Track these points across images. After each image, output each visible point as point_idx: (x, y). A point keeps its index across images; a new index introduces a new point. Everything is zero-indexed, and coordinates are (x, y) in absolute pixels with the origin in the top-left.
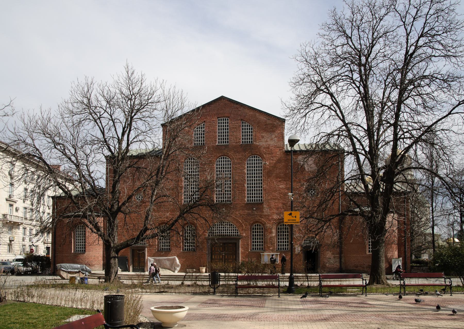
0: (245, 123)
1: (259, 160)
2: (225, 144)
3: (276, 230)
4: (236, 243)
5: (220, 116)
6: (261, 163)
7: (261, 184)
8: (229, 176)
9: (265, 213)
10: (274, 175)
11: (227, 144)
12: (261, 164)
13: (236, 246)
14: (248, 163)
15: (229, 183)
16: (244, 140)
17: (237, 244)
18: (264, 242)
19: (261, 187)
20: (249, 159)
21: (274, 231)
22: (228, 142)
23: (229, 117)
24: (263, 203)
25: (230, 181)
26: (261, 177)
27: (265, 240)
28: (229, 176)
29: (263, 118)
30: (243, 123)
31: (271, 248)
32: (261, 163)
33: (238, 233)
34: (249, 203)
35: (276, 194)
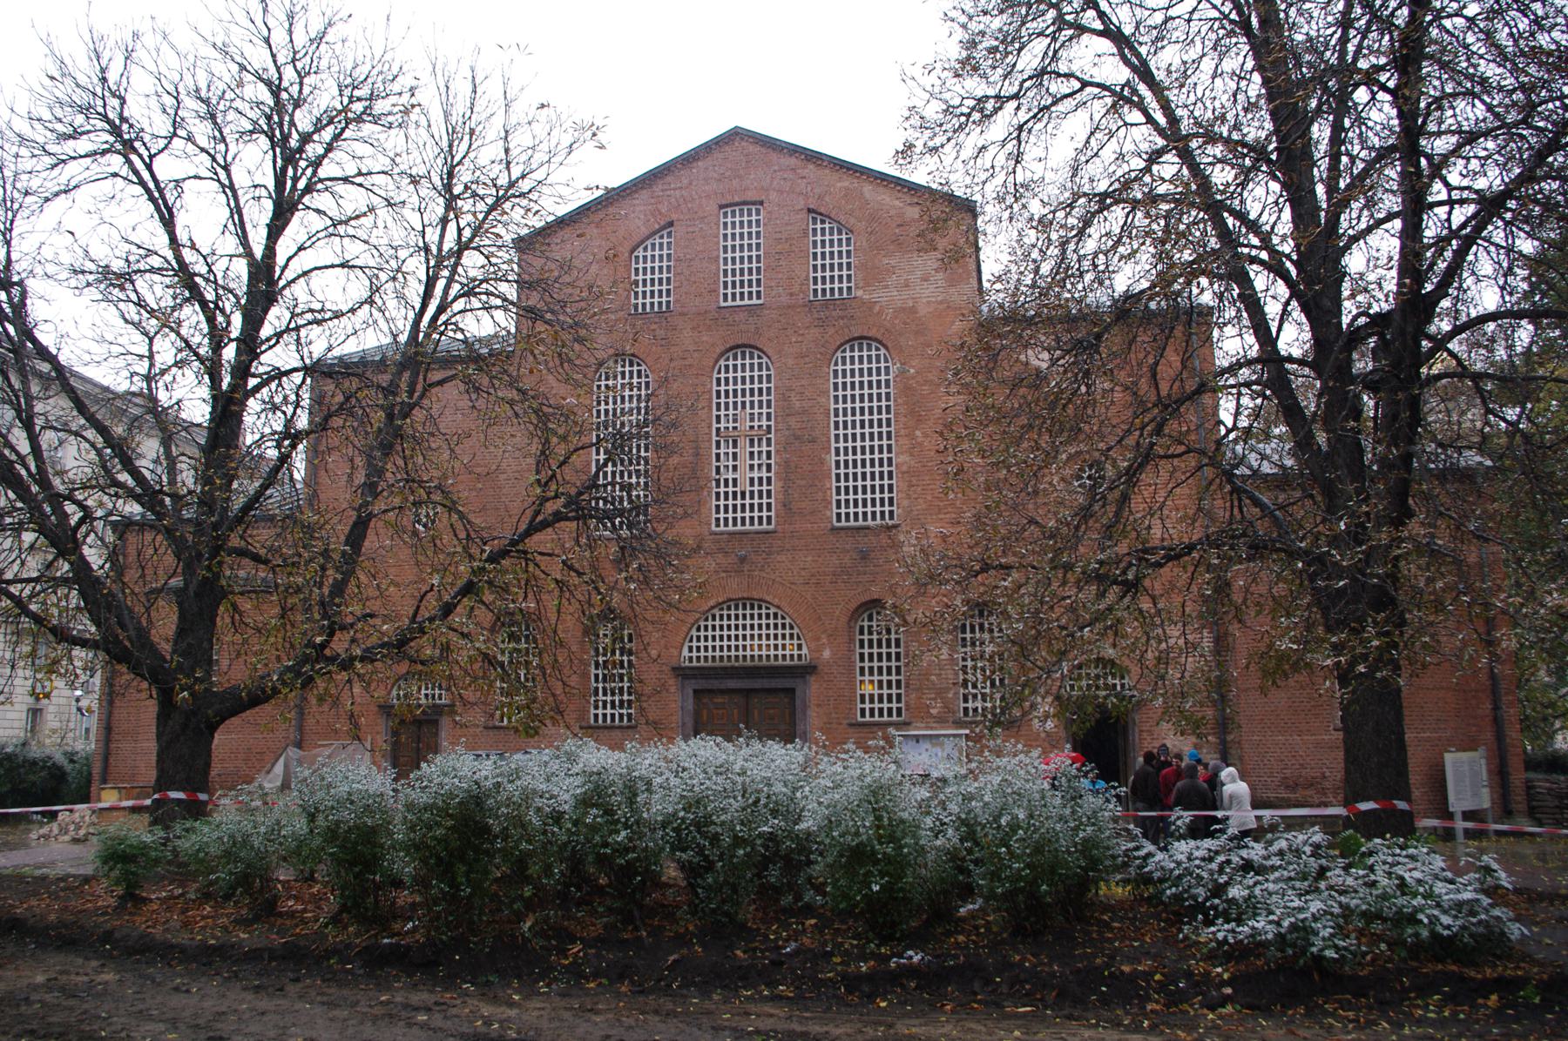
0: (823, 222)
1: (878, 356)
2: (746, 302)
4: (792, 691)
5: (729, 199)
8: (764, 423)
11: (755, 301)
12: (887, 374)
13: (793, 699)
15: (765, 449)
16: (819, 287)
17: (798, 693)
18: (907, 686)
20: (839, 354)
22: (759, 297)
23: (761, 203)
25: (769, 445)
28: (764, 423)
30: (815, 223)
32: (887, 368)
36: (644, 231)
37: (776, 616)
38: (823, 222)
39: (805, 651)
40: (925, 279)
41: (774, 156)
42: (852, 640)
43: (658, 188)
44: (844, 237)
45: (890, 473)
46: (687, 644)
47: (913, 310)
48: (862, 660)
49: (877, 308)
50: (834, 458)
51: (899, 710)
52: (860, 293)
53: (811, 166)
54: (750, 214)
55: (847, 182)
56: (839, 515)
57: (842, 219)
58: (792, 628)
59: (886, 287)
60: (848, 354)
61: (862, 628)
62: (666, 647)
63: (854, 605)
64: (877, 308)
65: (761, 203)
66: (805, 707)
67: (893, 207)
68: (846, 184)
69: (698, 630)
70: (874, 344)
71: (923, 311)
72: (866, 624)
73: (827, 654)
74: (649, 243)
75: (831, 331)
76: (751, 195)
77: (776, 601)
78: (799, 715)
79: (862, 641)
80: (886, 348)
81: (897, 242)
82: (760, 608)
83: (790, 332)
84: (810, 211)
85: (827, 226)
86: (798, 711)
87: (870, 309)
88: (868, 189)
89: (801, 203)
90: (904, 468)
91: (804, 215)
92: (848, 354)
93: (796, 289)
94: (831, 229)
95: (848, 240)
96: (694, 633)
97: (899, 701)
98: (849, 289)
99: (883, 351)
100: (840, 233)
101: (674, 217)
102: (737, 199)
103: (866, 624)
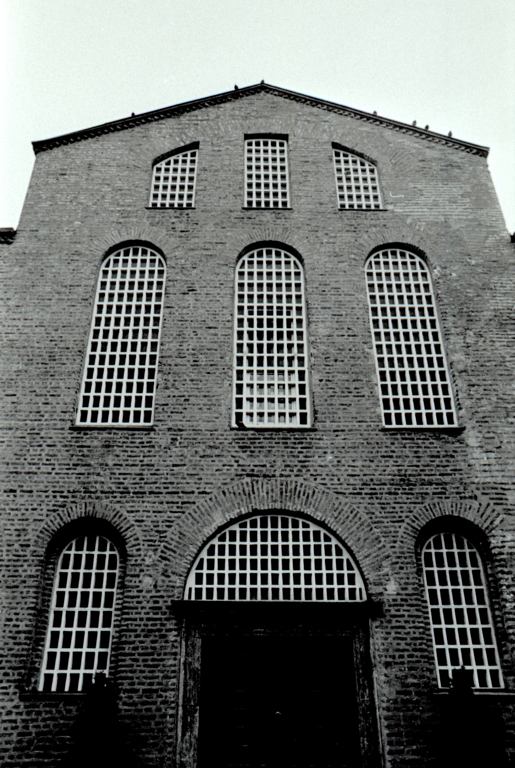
9: (481, 478)
10: (488, 314)
20: (372, 259)
24: (461, 430)
33: (352, 580)
36: (168, 147)
37: (317, 535)
39: (359, 584)
42: (419, 572)
43: (185, 118)
46: (194, 572)
47: (446, 224)
49: (409, 221)
50: (376, 356)
52: (390, 207)
53: (333, 115)
56: (388, 417)
58: (339, 552)
61: (428, 556)
62: (165, 574)
65: (285, 137)
68: (366, 129)
69: (211, 552)
73: (392, 588)
74: (172, 159)
77: (319, 516)
82: (295, 524)
83: (319, 234)
89: (325, 137)
90: (461, 367)
93: (325, 199)
96: (204, 555)
101: (200, 139)
102: (262, 131)
103: (433, 551)
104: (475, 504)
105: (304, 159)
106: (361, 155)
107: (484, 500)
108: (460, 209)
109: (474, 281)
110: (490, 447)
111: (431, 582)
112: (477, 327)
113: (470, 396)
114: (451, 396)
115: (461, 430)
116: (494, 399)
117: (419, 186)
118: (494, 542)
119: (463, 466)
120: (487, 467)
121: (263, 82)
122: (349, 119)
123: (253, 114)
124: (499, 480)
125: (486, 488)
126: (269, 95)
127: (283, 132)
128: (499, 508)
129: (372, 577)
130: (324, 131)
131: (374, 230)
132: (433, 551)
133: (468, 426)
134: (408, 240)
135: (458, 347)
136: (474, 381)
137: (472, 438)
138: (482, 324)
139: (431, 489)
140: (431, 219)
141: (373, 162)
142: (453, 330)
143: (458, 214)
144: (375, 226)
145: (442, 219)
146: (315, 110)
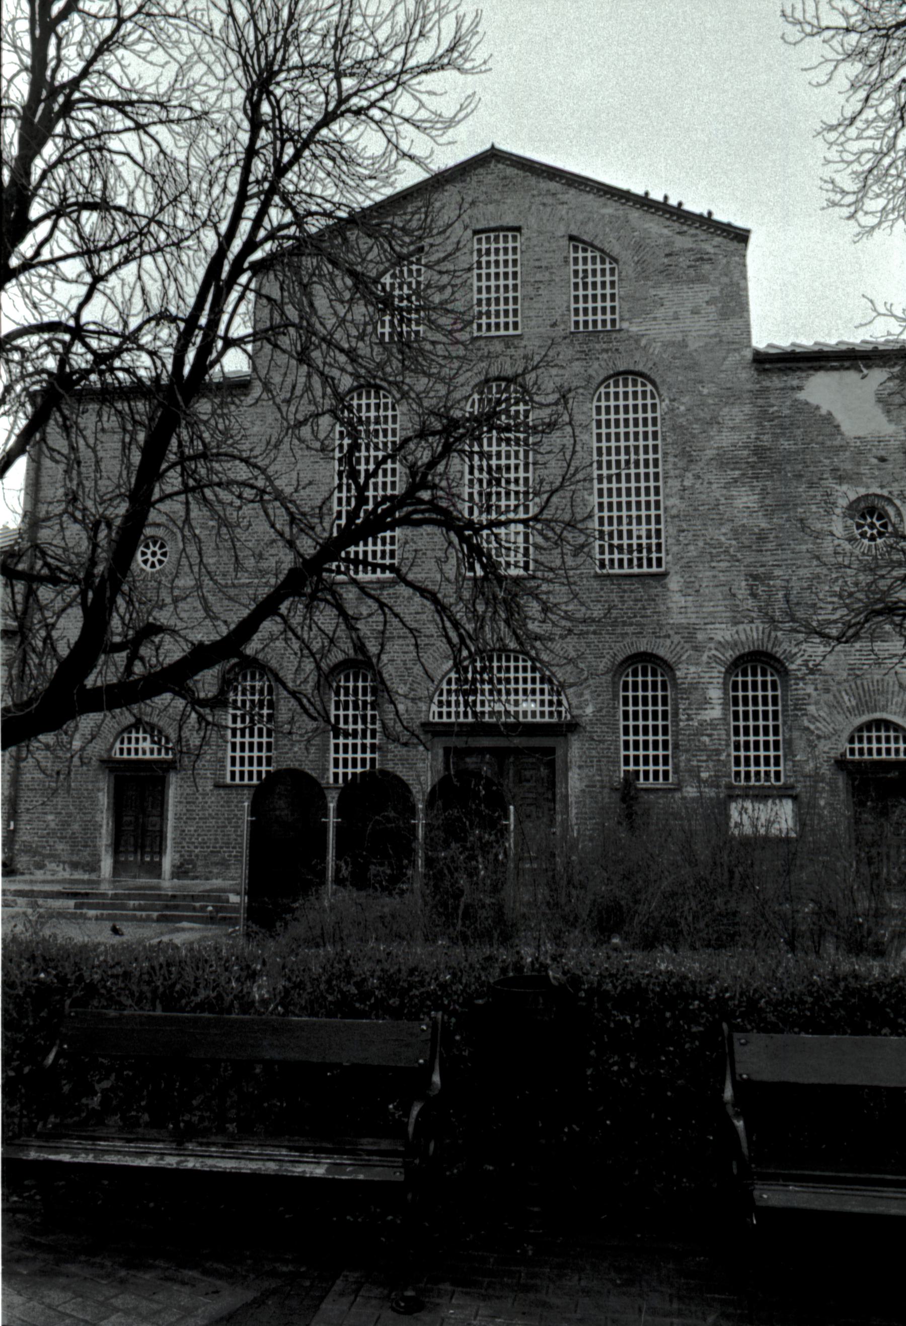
1: (644, 393)
2: (502, 332)
3: (725, 692)
4: (552, 751)
6: (654, 406)
7: (657, 493)
10: (710, 453)
11: (511, 332)
14: (598, 408)
17: (559, 752)
18: (676, 746)
19: (657, 507)
20: (602, 390)
21: (715, 694)
24: (665, 575)
26: (656, 465)
27: (676, 733)
29: (656, 228)
31: (704, 775)
32: (654, 406)
34: (609, 576)
35: (721, 534)
38: (585, 250)
40: (695, 312)
41: (533, 180)
42: (615, 696)
44: (607, 266)
45: (658, 517)
47: (683, 344)
48: (626, 718)
51: (666, 773)
52: (625, 325)
53: (572, 191)
54: (506, 241)
55: (610, 209)
57: (607, 247)
59: (655, 319)
60: (612, 390)
61: (626, 684)
63: (620, 658)
64: (643, 342)
65: (518, 229)
66: (567, 769)
67: (661, 236)
70: (640, 380)
71: (693, 345)
72: (630, 679)
73: (589, 710)
75: (596, 365)
76: (509, 220)
78: (558, 779)
79: (626, 699)
80: (653, 383)
81: (666, 272)
84: (572, 238)
85: (589, 255)
86: (558, 772)
87: (637, 341)
88: (635, 215)
89: (561, 230)
90: (674, 512)
91: (564, 242)
92: (612, 390)
94: (594, 259)
95: (612, 270)
97: (666, 763)
98: (613, 321)
99: (649, 387)
100: (603, 262)
102: (493, 224)
104: (668, 642)
105: (537, 264)
106: (602, 251)
107: (676, 639)
108: (703, 322)
109: (702, 415)
110: (689, 591)
111: (626, 703)
112: (696, 468)
113: (678, 542)
114: (663, 541)
115: (665, 575)
116: (701, 544)
117: (661, 293)
118: (678, 674)
119: (663, 608)
120: (683, 610)
121: (493, 147)
122: (591, 196)
123: (482, 198)
124: (693, 621)
125: (678, 628)
126: (500, 166)
127: (516, 224)
128: (687, 646)
129: (574, 702)
130: (561, 219)
131: (605, 356)
132: (630, 679)
133: (672, 572)
134: (640, 368)
135: (674, 490)
136: (685, 527)
137: (674, 583)
138: (701, 464)
139: (630, 630)
140: (668, 338)
141: (615, 260)
142: (672, 473)
143: (698, 329)
144: (607, 351)
145: (679, 337)
146: (553, 186)
